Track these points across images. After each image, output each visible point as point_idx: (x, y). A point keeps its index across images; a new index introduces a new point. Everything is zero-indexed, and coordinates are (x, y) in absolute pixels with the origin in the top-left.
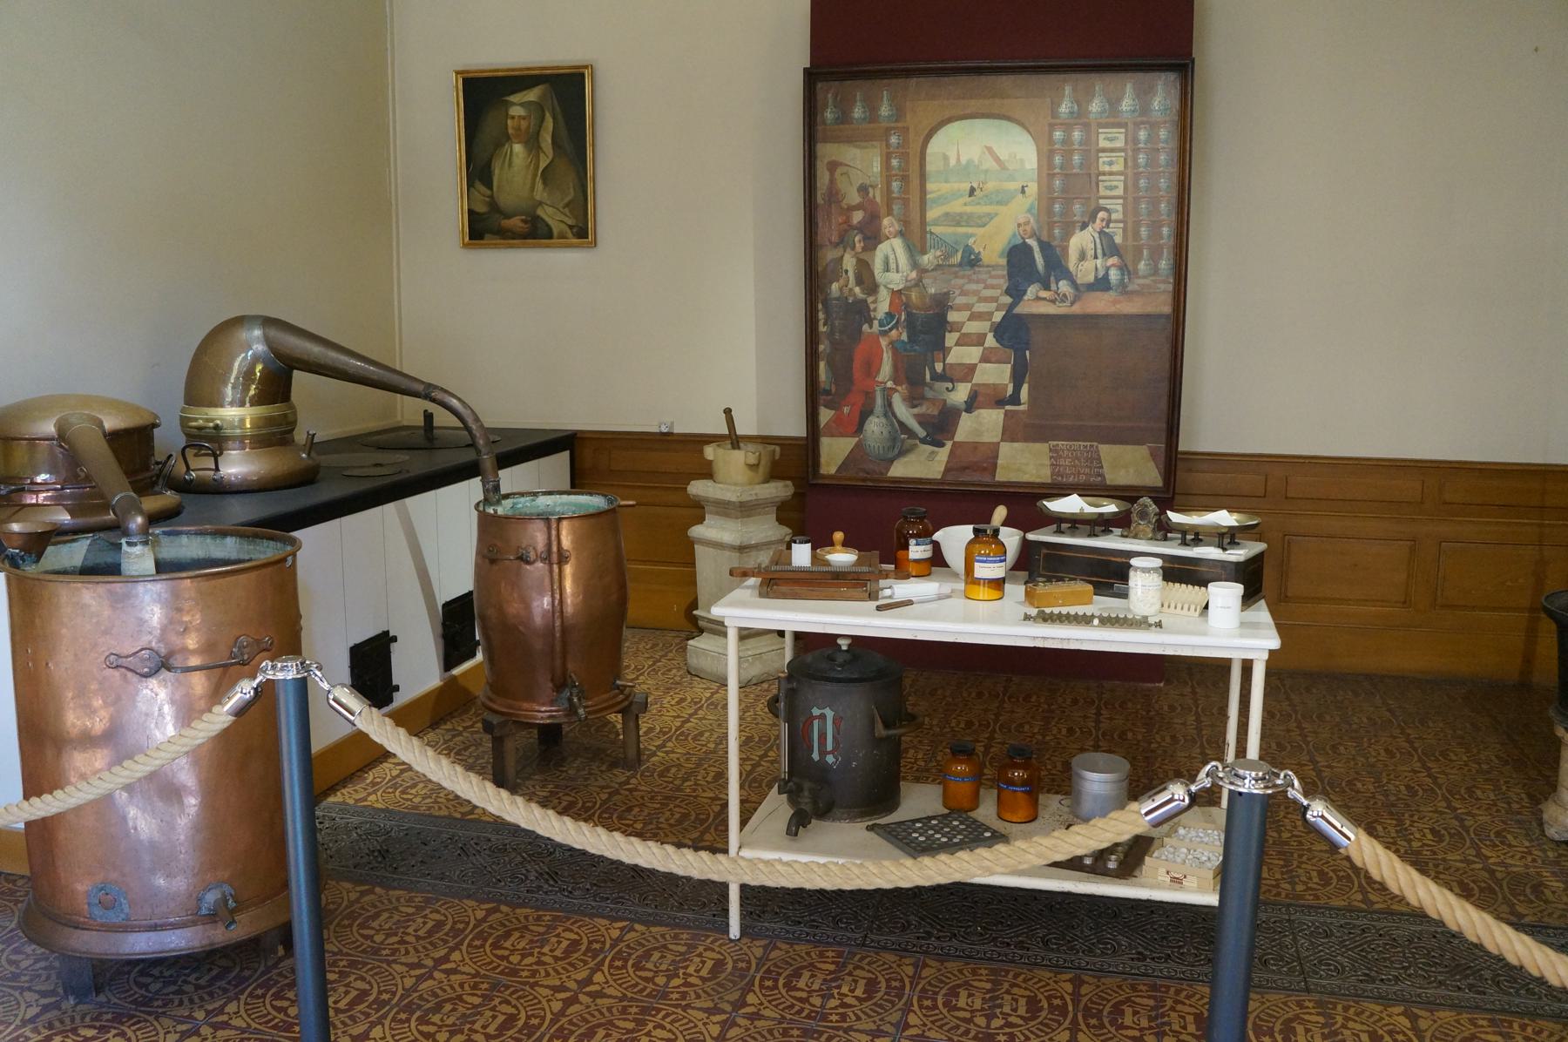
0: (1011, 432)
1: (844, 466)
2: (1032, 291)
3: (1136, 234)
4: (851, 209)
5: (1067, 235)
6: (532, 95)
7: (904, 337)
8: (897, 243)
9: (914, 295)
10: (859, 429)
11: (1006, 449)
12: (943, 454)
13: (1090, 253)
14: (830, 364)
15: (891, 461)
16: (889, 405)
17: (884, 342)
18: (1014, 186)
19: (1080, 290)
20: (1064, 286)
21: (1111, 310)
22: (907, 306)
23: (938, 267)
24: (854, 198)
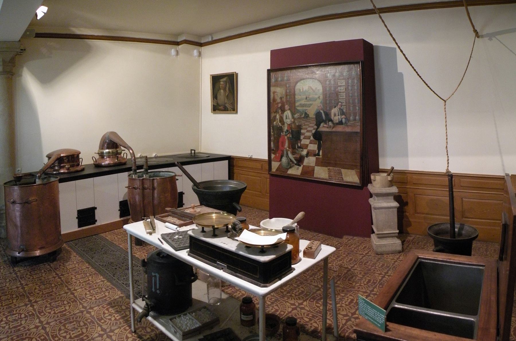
0: (317, 164)
1: (277, 170)
2: (322, 124)
3: (349, 109)
4: (278, 103)
5: (331, 109)
6: (224, 79)
7: (291, 136)
8: (289, 112)
9: (293, 126)
10: (281, 160)
11: (317, 168)
12: (301, 168)
13: (337, 114)
14: (274, 143)
15: (288, 169)
16: (287, 154)
17: (286, 137)
18: (317, 96)
19: (336, 124)
20: (330, 123)
21: (343, 130)
22: (291, 128)
23: (299, 118)
24: (279, 100)
